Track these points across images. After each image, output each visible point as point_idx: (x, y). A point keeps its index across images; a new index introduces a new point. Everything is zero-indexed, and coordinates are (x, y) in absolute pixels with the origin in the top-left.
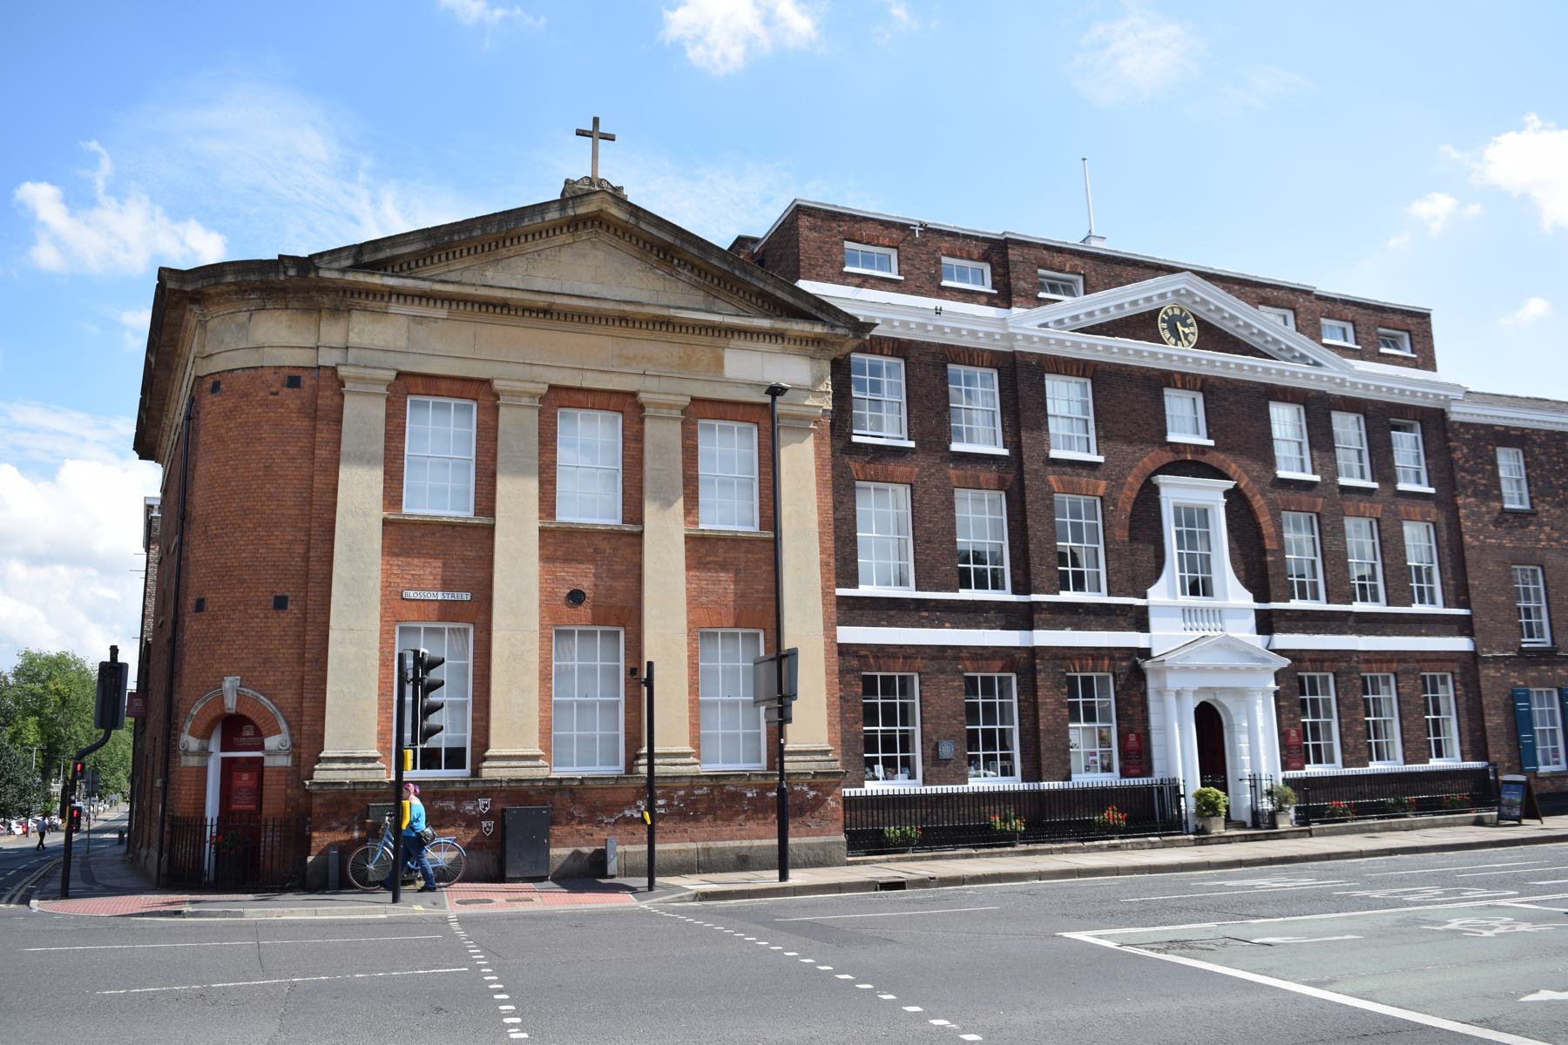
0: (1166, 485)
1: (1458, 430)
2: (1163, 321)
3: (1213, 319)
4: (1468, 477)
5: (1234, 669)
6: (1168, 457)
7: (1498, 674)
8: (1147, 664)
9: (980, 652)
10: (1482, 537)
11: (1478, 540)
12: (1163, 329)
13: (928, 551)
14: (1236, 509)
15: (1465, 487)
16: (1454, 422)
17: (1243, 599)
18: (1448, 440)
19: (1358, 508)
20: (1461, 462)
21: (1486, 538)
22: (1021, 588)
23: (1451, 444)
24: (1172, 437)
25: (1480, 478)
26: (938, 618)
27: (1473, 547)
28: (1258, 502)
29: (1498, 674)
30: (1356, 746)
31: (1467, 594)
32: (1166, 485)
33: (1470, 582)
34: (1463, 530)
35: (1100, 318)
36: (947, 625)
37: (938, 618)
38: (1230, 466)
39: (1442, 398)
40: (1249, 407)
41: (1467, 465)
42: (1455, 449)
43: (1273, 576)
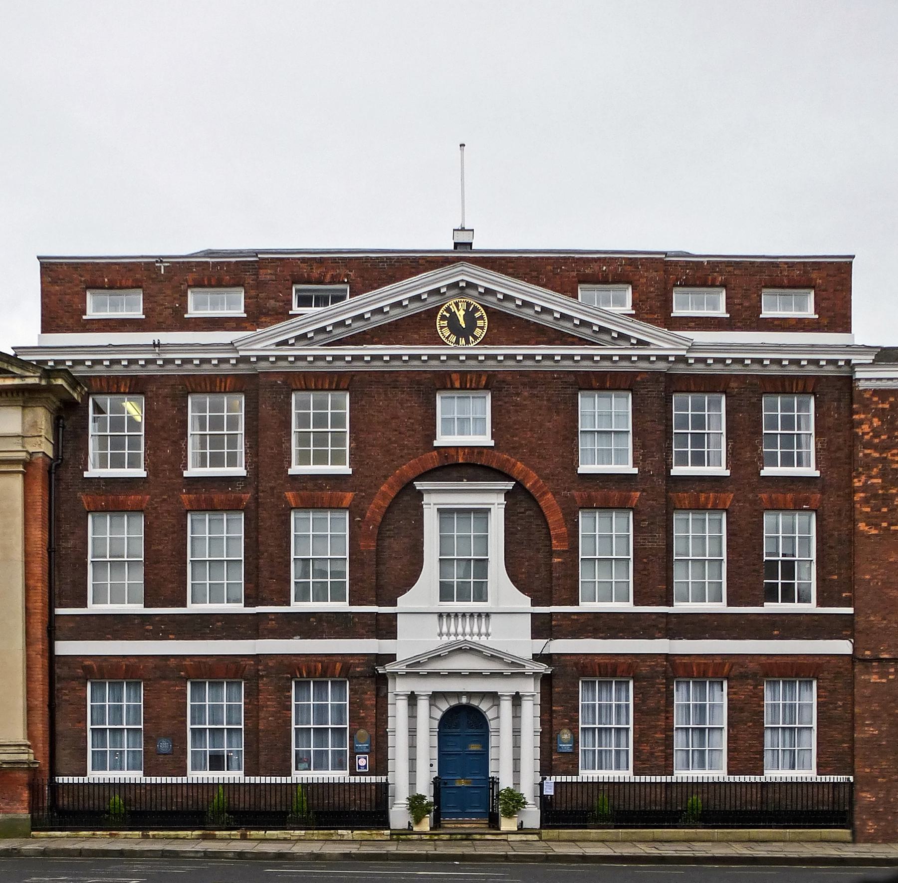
0: (429, 491)
1: (869, 399)
2: (443, 318)
3: (509, 308)
4: (877, 455)
5: (494, 675)
6: (432, 461)
7: (884, 681)
8: (390, 668)
9: (204, 660)
10: (884, 524)
11: (877, 526)
12: (442, 328)
13: (156, 572)
14: (522, 510)
15: (868, 467)
16: (865, 390)
17: (524, 602)
18: (852, 412)
19: (697, 499)
20: (867, 437)
21: (890, 524)
22: (251, 601)
23: (856, 417)
24: (441, 440)
25: (893, 455)
26: (162, 631)
27: (869, 537)
28: (548, 501)
29: (884, 681)
30: (652, 754)
31: (851, 589)
32: (429, 491)
33: (858, 576)
34: (857, 517)
35: (359, 327)
36: (171, 636)
37: (162, 631)
38: (514, 465)
39: (841, 363)
40: (548, 400)
41: (876, 441)
42: (861, 423)
43: (558, 578)
